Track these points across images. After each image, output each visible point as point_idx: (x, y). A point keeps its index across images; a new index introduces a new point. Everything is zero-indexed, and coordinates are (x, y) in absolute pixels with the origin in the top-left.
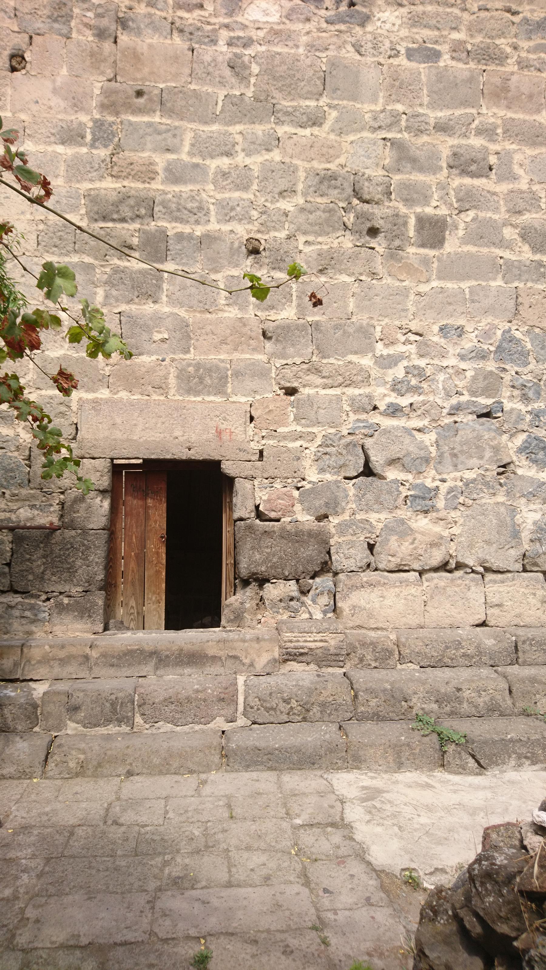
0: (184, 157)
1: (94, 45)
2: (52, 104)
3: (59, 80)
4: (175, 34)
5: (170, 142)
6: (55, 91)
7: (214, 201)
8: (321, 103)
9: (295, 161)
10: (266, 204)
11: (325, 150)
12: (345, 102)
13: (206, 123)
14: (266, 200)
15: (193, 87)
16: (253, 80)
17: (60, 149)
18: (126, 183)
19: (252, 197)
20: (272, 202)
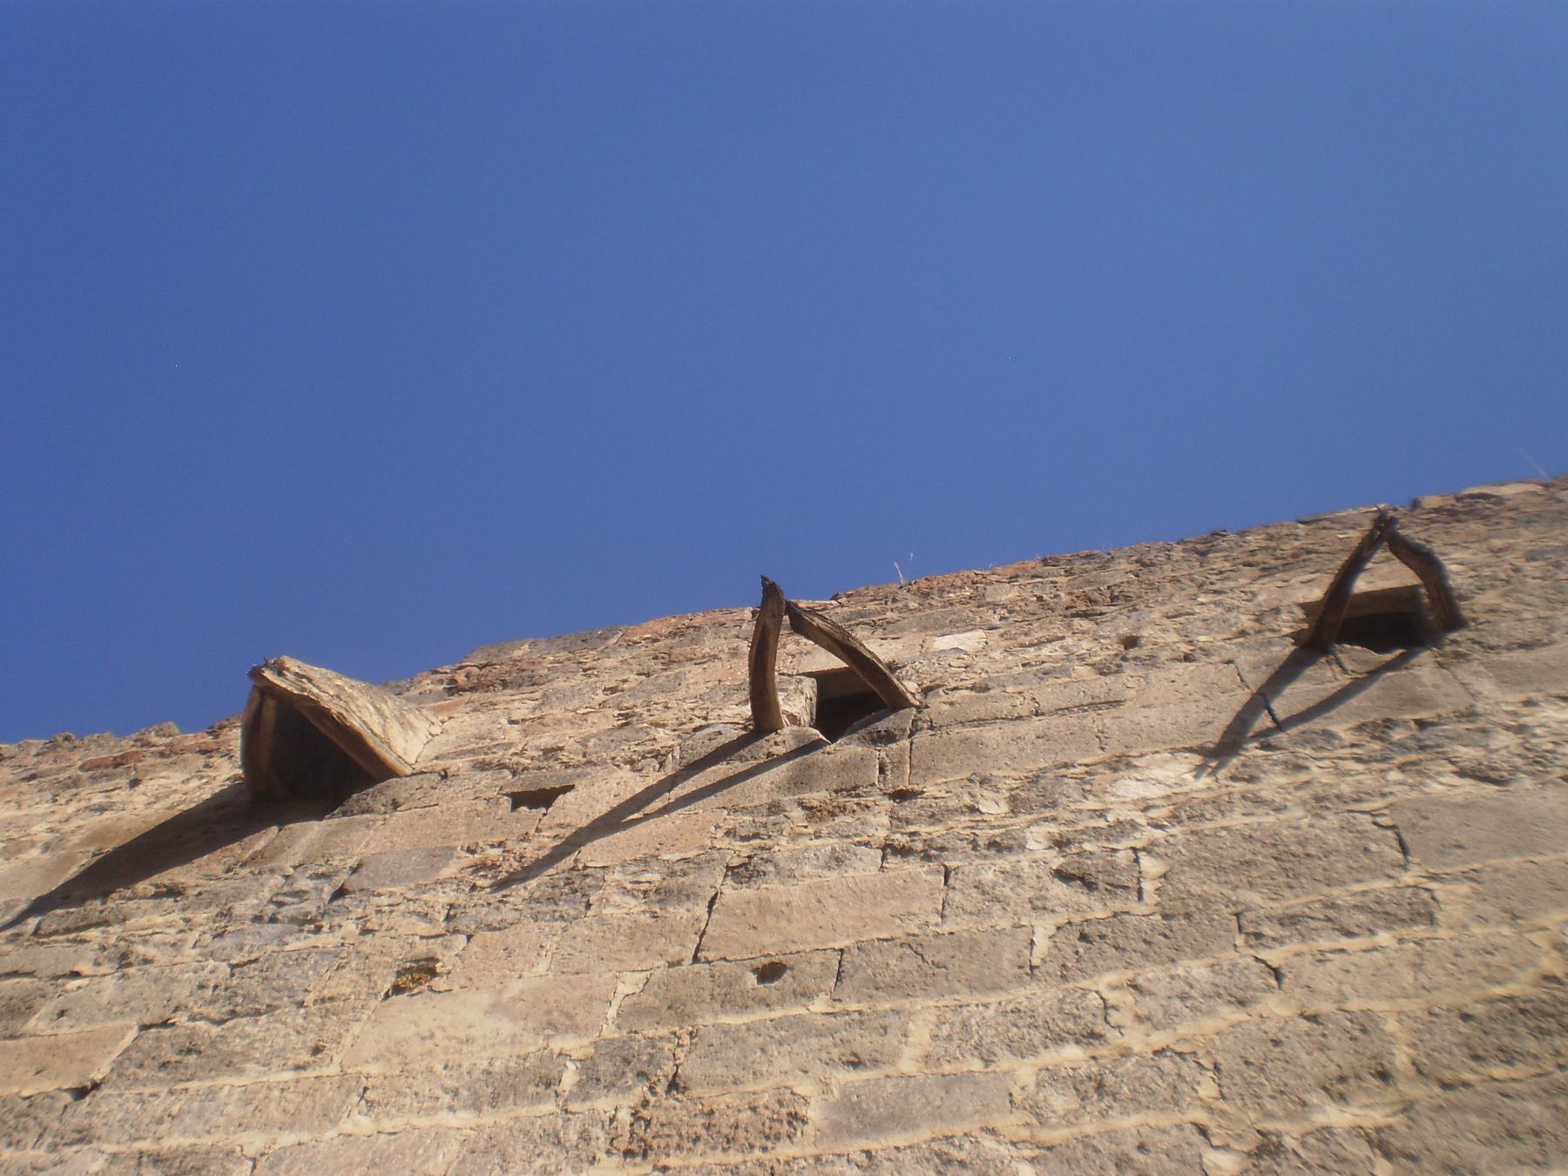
0: (907, 1065)
1: (645, 919)
2: (473, 1032)
3: (515, 987)
4: (893, 861)
5: (863, 1043)
6: (495, 1009)
7: (1027, 1153)
8: (1408, 878)
9: (1355, 1005)
10: (1268, 1126)
11: (1471, 960)
12: (1491, 862)
13: (996, 988)
14: (1269, 1115)
15: (945, 929)
16: (1148, 886)
17: (464, 1119)
18: (664, 1161)
19: (1201, 1117)
20: (1290, 1116)
